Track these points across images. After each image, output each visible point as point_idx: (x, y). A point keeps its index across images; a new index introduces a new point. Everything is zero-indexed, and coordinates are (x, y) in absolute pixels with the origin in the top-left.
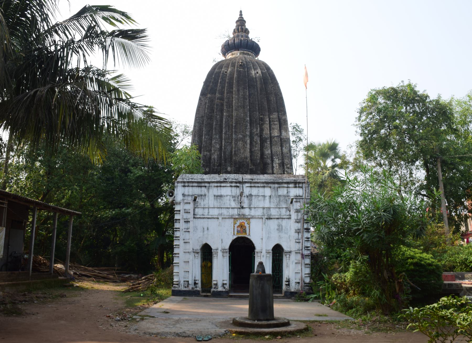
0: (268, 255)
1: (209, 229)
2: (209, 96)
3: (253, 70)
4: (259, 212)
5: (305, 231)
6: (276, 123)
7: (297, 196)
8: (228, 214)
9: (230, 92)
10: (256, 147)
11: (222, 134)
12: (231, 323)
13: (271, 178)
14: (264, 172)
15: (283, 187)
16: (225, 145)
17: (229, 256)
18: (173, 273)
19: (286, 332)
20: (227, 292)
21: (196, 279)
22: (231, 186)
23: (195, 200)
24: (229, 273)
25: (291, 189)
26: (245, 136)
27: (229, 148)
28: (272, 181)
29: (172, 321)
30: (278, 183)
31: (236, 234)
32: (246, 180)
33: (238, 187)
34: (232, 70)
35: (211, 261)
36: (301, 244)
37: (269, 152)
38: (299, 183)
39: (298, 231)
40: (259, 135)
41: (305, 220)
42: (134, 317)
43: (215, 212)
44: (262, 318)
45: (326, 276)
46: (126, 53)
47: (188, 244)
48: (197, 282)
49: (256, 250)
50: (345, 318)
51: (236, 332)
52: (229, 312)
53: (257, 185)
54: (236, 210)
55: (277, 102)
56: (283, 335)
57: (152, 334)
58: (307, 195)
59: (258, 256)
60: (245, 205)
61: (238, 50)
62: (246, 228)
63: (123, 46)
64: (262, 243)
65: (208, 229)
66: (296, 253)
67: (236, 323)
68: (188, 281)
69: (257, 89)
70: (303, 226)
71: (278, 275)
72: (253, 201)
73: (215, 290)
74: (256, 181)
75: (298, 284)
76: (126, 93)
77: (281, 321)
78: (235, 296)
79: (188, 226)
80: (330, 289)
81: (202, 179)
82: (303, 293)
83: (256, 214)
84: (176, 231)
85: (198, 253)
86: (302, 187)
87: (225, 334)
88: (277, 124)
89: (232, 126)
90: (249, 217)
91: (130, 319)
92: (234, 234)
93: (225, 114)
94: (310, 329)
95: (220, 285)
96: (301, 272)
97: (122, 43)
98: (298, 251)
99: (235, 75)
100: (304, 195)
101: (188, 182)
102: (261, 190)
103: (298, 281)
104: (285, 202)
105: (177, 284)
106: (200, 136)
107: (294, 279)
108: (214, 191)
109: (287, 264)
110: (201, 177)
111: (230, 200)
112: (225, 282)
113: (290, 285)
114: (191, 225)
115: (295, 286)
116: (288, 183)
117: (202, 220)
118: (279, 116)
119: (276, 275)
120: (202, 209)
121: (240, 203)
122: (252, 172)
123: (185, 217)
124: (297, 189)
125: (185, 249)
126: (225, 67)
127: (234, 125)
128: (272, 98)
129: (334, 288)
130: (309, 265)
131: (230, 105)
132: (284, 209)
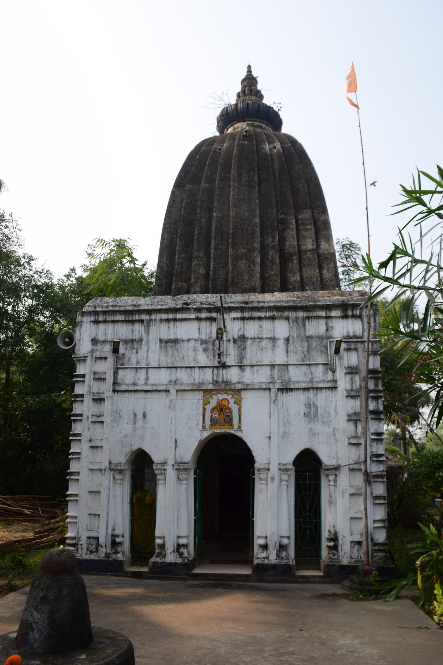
0: (285, 477)
2: (188, 187)
3: (267, 143)
4: (262, 376)
6: (309, 227)
7: (349, 337)
8: (191, 381)
9: (226, 178)
10: (272, 269)
11: (211, 248)
13: (289, 299)
16: (215, 268)
17: (195, 479)
20: (188, 566)
21: (117, 532)
22: (199, 319)
23: (116, 350)
26: (251, 251)
27: (222, 273)
30: (305, 308)
31: (207, 427)
34: (230, 145)
36: (362, 447)
37: (297, 277)
38: (354, 306)
39: (354, 419)
40: (277, 248)
41: (371, 391)
43: (161, 378)
47: (99, 450)
48: (117, 540)
49: (256, 465)
53: (256, 314)
54: (209, 372)
55: (309, 193)
58: (372, 332)
59: (261, 479)
60: (230, 360)
61: (244, 121)
62: (231, 412)
64: (270, 447)
65: (144, 416)
66: (352, 470)
68: (97, 538)
69: (274, 173)
70: (367, 406)
71: (310, 523)
72: (248, 350)
73: (159, 560)
75: (357, 547)
78: (204, 575)
79: (102, 410)
81: (135, 306)
83: (256, 381)
84: (75, 421)
86: (360, 317)
88: (310, 229)
89: (228, 234)
90: (239, 386)
92: (204, 427)
95: (170, 547)
96: (363, 516)
98: (357, 466)
99: (235, 152)
100: (366, 335)
101: (104, 313)
102: (267, 325)
103: (357, 538)
104: (322, 352)
105: (73, 545)
107: (347, 534)
109: (330, 496)
111: (195, 350)
112: (183, 541)
113: (340, 548)
114: (107, 406)
115: (352, 552)
116: (328, 307)
117: (132, 396)
118: (313, 216)
120: (133, 371)
121: (219, 355)
123: (95, 390)
124: (350, 321)
125: (93, 463)
127: (231, 232)
130: (384, 498)
132: (321, 368)
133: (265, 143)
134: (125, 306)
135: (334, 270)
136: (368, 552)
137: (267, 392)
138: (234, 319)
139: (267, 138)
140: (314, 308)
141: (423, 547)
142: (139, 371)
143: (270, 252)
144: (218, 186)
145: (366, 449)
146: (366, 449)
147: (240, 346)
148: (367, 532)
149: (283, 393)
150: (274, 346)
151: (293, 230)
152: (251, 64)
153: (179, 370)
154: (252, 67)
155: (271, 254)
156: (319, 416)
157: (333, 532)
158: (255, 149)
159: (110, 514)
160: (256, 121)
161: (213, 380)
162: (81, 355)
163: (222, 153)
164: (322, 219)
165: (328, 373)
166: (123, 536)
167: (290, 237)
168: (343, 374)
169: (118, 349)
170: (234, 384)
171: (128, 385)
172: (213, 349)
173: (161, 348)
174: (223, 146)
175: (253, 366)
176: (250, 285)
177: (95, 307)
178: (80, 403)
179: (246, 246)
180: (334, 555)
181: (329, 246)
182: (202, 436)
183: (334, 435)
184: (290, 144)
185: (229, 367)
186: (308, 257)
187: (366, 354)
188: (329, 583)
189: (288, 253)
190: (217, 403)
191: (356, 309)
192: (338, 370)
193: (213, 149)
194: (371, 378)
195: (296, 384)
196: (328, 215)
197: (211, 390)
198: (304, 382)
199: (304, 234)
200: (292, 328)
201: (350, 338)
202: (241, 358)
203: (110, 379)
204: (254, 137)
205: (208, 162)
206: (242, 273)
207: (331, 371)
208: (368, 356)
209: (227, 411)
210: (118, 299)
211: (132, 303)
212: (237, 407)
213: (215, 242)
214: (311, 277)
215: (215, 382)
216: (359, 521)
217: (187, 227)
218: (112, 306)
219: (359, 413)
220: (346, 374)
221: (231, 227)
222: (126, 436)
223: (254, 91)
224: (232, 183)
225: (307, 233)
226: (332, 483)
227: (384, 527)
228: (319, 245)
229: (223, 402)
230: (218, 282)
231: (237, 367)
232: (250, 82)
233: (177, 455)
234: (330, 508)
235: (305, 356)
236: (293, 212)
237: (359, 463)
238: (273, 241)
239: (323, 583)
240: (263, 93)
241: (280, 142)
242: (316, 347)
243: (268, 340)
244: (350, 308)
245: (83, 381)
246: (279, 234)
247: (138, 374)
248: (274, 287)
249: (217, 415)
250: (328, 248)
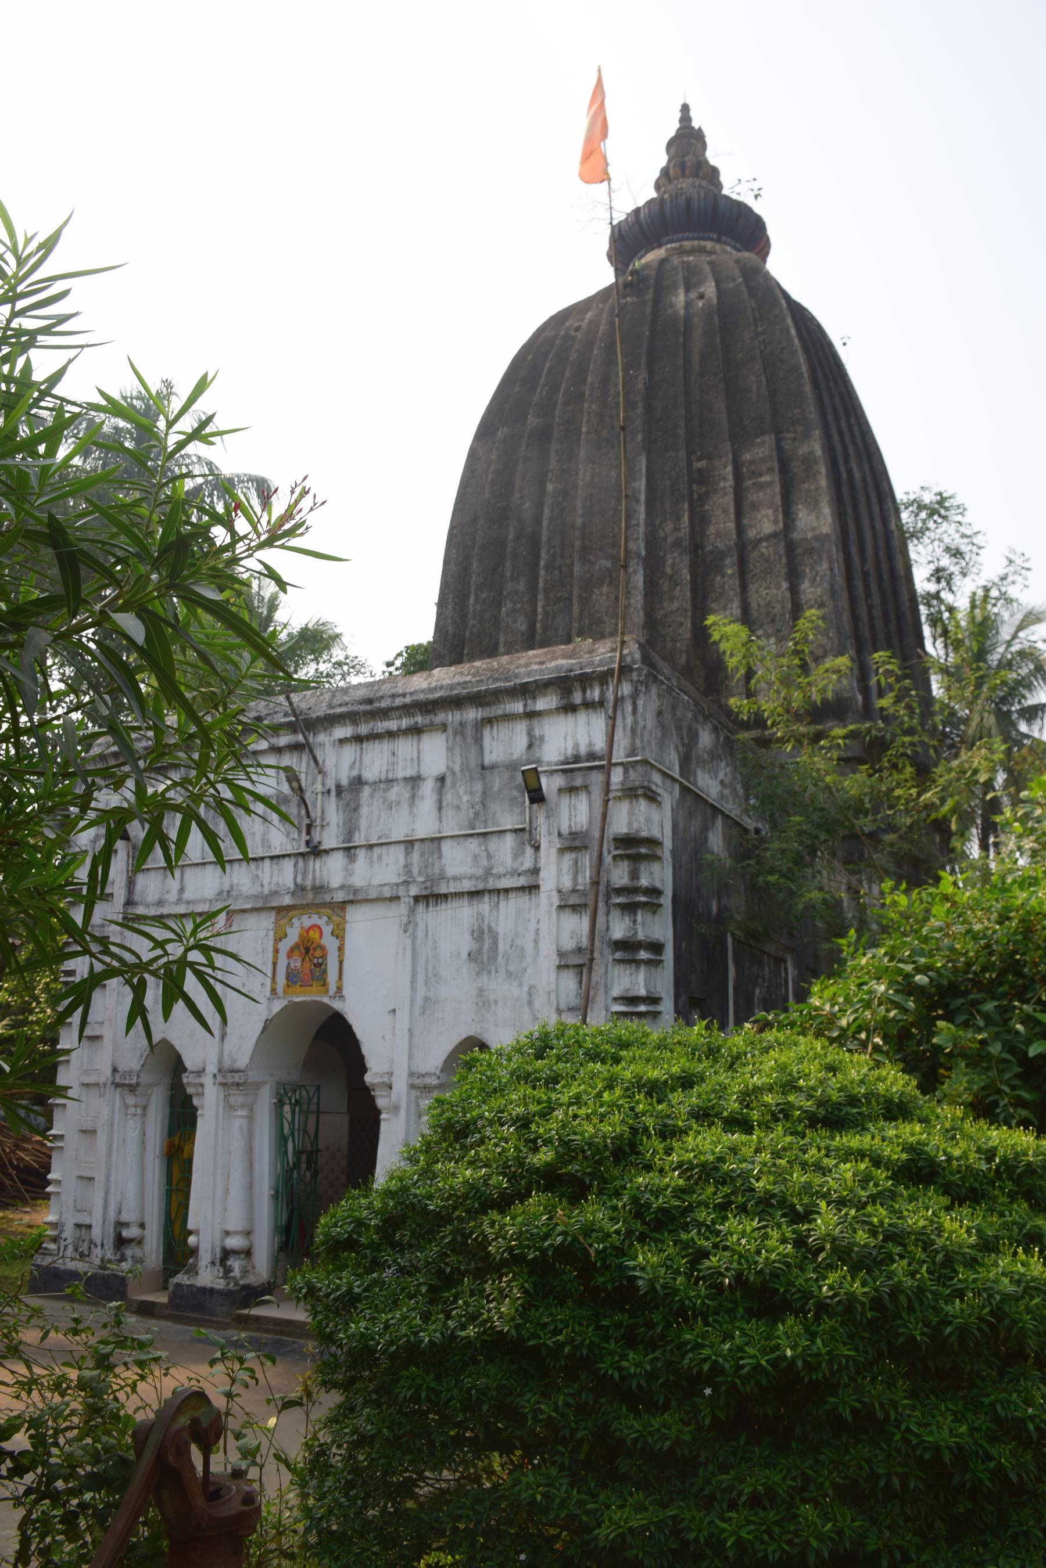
4: (383, 871)
6: (766, 478)
8: (255, 890)
10: (671, 599)
16: (546, 614)
21: (125, 1217)
30: (477, 699)
31: (280, 991)
40: (686, 543)
41: (619, 891)
48: (126, 1233)
53: (382, 726)
54: (288, 865)
60: (330, 838)
61: (660, 246)
62: (324, 956)
69: (687, 361)
72: (364, 810)
90: (340, 896)
92: (274, 991)
93: (550, 487)
102: (405, 747)
116: (526, 691)
118: (779, 449)
124: (582, 717)
128: (753, 378)
132: (509, 840)
133: (676, 289)
135: (828, 578)
138: (342, 741)
147: (348, 804)
149: (427, 905)
150: (413, 797)
151: (725, 494)
154: (691, 107)
155: (670, 561)
156: (500, 959)
159: (113, 1179)
160: (687, 239)
161: (296, 884)
164: (800, 452)
165: (524, 853)
166: (142, 1226)
168: (553, 852)
175: (371, 847)
181: (818, 517)
182: (270, 1011)
183: (530, 1003)
185: (326, 852)
186: (762, 555)
189: (712, 552)
190: (300, 936)
191: (591, 687)
194: (622, 857)
195: (451, 883)
197: (289, 908)
199: (754, 498)
202: (350, 829)
205: (547, 366)
207: (533, 846)
209: (318, 953)
212: (337, 943)
214: (769, 604)
215: (301, 889)
220: (562, 851)
221: (580, 512)
224: (586, 405)
225: (761, 494)
228: (794, 521)
229: (311, 933)
231: (341, 852)
232: (687, 143)
233: (226, 1054)
235: (477, 814)
236: (729, 448)
238: (677, 529)
242: (500, 791)
244: (577, 685)
248: (675, 641)
250: (815, 524)
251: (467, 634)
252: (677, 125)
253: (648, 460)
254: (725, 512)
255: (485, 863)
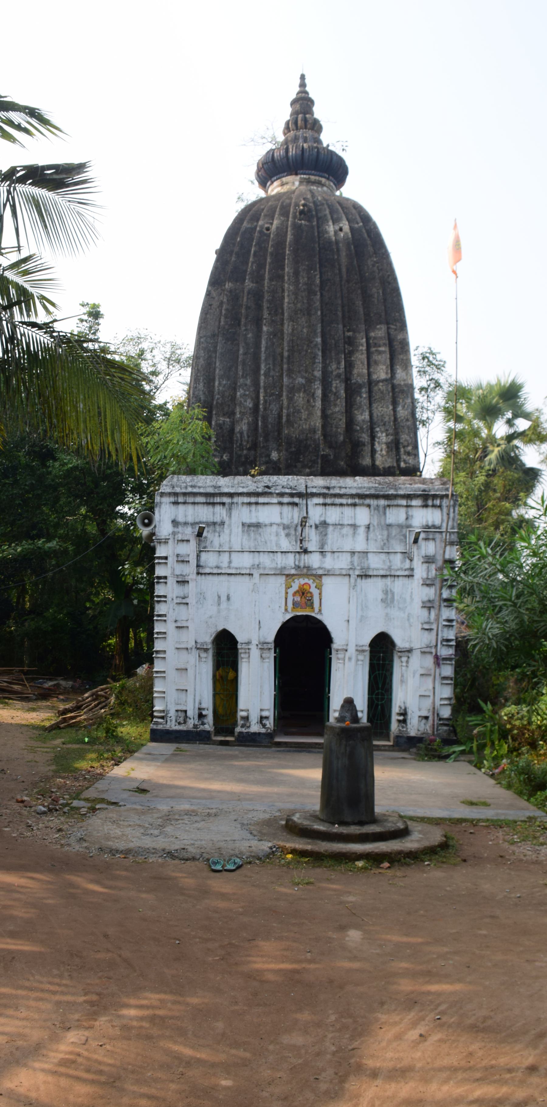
0: (361, 657)
1: (232, 599)
2: (228, 285)
3: (331, 223)
4: (342, 563)
5: (444, 604)
6: (382, 349)
7: (428, 527)
8: (273, 565)
9: (278, 277)
10: (335, 405)
11: (260, 374)
12: (282, 826)
13: (371, 485)
14: (355, 470)
15: (398, 506)
16: (265, 401)
17: (275, 657)
18: (151, 692)
19: (400, 853)
22: (281, 504)
23: (200, 534)
24: (273, 693)
25: (414, 509)
26: (310, 381)
27: (274, 408)
28: (373, 492)
29: (155, 815)
30: (387, 497)
32: (314, 490)
33: (296, 504)
34: (282, 224)
35: (234, 666)
36: (434, 633)
37: (366, 416)
38: (435, 497)
40: (343, 377)
42: (75, 803)
43: (243, 561)
44: (349, 819)
45: (488, 707)
46: (44, 221)
47: (184, 631)
49: (334, 646)
50: (528, 814)
51: (293, 851)
52: (276, 790)
53: (338, 501)
54: (291, 556)
55: (385, 300)
56: (394, 859)
57: (117, 851)
58: (450, 523)
59: (338, 659)
60: (312, 545)
61: (296, 174)
62: (312, 596)
63: (36, 204)
64: (348, 630)
65: (228, 598)
67: (292, 828)
69: (340, 269)
70: (441, 594)
71: (383, 699)
72: (330, 536)
74: (337, 491)
75: (424, 721)
76: (42, 298)
77: (390, 826)
78: (286, 744)
79: (186, 592)
80: (496, 736)
81: (215, 487)
82: (435, 741)
83: (336, 567)
84: (159, 602)
85: (206, 650)
86: (440, 507)
87: (271, 854)
88: (384, 352)
89: (282, 357)
90: (320, 572)
91: (66, 809)
92: (286, 610)
93: (265, 329)
94: (451, 843)
96: (431, 695)
97: (33, 197)
99: (289, 237)
101: (185, 494)
102: (348, 511)
103: (425, 713)
104: (401, 540)
106: (209, 381)
108: (244, 514)
109: (402, 676)
110: (214, 483)
111: (277, 535)
113: (408, 722)
114: (191, 589)
115: (419, 725)
116: (409, 497)
117: (216, 578)
118: (389, 334)
119: (377, 699)
120: (216, 555)
121: (301, 541)
122: (328, 470)
123: (178, 572)
124: (430, 510)
126: (265, 216)
127: (286, 354)
128: (374, 290)
129: (504, 734)
130: (451, 679)
131: (277, 308)
132: (399, 556)
134: (205, 487)
135: (411, 407)
136: (433, 725)
137: (347, 578)
138: (316, 504)
139: (331, 213)
140: (395, 497)
141: (482, 720)
142: (221, 553)
143: (334, 382)
144: (269, 287)
145: (437, 635)
146: (437, 635)
148: (434, 708)
150: (354, 533)
151: (362, 354)
152: (304, 73)
153: (262, 554)
157: (403, 708)
158: (316, 234)
162: (163, 537)
163: (272, 236)
167: (359, 363)
168: (420, 563)
169: (202, 533)
170: (315, 569)
171: (212, 568)
172: (295, 534)
173: (243, 531)
174: (272, 224)
175: (334, 552)
176: (310, 425)
177: (173, 487)
178: (163, 585)
179: (304, 374)
180: (403, 727)
181: (407, 375)
183: (408, 620)
184: (361, 224)
185: (311, 552)
186: (380, 389)
187: (443, 545)
188: (399, 751)
189: (355, 383)
192: (416, 559)
193: (258, 229)
196: (407, 333)
197: (293, 575)
198: (383, 569)
200: (373, 516)
201: (429, 528)
203: (193, 562)
204: (314, 213)
206: (299, 410)
208: (445, 547)
209: (309, 595)
210: (195, 478)
211: (211, 484)
212: (318, 591)
213: (265, 366)
214: (382, 415)
216: (427, 698)
217: (229, 343)
218: (192, 486)
219: (433, 601)
221: (286, 348)
222: (211, 617)
223: (310, 122)
225: (380, 357)
226: (404, 664)
227: (450, 705)
228: (395, 374)
230: (270, 420)
231: (318, 553)
234: (401, 686)
235: (385, 544)
236: (364, 328)
237: (431, 647)
239: (393, 751)
240: (322, 123)
241: (348, 220)
243: (349, 527)
245: (166, 563)
246: (345, 358)
247: (221, 557)
248: (337, 428)
249: (299, 599)
250: (405, 378)
251: (215, 403)
252: (297, 89)
253: (322, 326)
254: (362, 363)
255: (388, 564)
